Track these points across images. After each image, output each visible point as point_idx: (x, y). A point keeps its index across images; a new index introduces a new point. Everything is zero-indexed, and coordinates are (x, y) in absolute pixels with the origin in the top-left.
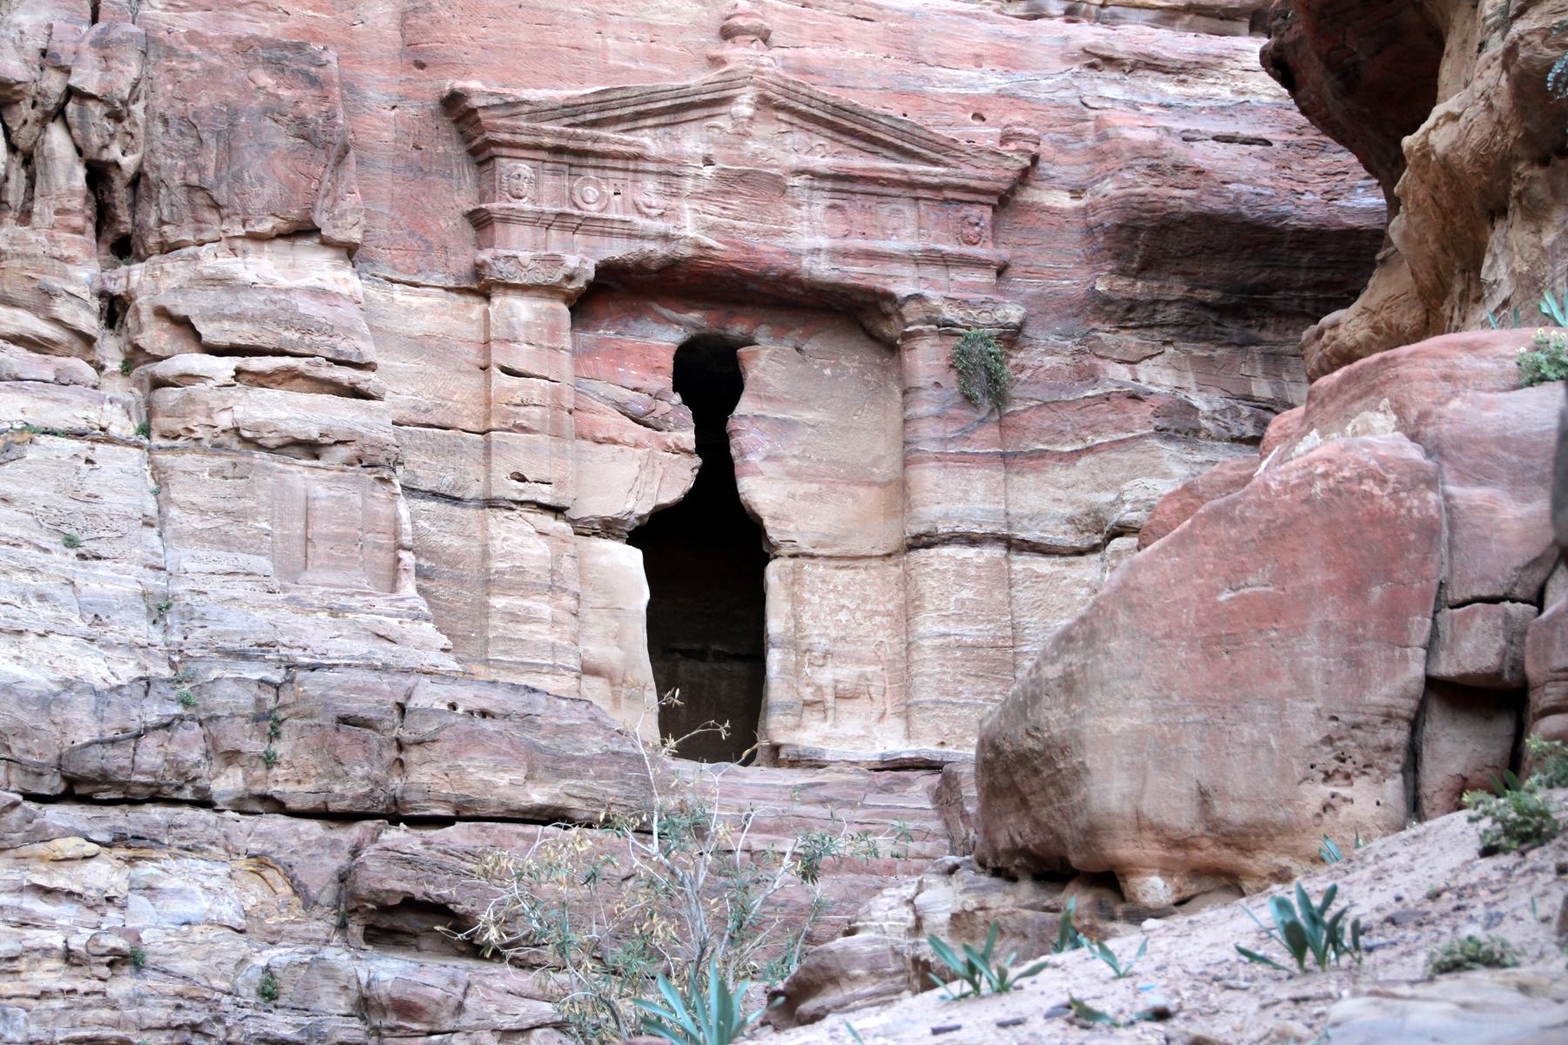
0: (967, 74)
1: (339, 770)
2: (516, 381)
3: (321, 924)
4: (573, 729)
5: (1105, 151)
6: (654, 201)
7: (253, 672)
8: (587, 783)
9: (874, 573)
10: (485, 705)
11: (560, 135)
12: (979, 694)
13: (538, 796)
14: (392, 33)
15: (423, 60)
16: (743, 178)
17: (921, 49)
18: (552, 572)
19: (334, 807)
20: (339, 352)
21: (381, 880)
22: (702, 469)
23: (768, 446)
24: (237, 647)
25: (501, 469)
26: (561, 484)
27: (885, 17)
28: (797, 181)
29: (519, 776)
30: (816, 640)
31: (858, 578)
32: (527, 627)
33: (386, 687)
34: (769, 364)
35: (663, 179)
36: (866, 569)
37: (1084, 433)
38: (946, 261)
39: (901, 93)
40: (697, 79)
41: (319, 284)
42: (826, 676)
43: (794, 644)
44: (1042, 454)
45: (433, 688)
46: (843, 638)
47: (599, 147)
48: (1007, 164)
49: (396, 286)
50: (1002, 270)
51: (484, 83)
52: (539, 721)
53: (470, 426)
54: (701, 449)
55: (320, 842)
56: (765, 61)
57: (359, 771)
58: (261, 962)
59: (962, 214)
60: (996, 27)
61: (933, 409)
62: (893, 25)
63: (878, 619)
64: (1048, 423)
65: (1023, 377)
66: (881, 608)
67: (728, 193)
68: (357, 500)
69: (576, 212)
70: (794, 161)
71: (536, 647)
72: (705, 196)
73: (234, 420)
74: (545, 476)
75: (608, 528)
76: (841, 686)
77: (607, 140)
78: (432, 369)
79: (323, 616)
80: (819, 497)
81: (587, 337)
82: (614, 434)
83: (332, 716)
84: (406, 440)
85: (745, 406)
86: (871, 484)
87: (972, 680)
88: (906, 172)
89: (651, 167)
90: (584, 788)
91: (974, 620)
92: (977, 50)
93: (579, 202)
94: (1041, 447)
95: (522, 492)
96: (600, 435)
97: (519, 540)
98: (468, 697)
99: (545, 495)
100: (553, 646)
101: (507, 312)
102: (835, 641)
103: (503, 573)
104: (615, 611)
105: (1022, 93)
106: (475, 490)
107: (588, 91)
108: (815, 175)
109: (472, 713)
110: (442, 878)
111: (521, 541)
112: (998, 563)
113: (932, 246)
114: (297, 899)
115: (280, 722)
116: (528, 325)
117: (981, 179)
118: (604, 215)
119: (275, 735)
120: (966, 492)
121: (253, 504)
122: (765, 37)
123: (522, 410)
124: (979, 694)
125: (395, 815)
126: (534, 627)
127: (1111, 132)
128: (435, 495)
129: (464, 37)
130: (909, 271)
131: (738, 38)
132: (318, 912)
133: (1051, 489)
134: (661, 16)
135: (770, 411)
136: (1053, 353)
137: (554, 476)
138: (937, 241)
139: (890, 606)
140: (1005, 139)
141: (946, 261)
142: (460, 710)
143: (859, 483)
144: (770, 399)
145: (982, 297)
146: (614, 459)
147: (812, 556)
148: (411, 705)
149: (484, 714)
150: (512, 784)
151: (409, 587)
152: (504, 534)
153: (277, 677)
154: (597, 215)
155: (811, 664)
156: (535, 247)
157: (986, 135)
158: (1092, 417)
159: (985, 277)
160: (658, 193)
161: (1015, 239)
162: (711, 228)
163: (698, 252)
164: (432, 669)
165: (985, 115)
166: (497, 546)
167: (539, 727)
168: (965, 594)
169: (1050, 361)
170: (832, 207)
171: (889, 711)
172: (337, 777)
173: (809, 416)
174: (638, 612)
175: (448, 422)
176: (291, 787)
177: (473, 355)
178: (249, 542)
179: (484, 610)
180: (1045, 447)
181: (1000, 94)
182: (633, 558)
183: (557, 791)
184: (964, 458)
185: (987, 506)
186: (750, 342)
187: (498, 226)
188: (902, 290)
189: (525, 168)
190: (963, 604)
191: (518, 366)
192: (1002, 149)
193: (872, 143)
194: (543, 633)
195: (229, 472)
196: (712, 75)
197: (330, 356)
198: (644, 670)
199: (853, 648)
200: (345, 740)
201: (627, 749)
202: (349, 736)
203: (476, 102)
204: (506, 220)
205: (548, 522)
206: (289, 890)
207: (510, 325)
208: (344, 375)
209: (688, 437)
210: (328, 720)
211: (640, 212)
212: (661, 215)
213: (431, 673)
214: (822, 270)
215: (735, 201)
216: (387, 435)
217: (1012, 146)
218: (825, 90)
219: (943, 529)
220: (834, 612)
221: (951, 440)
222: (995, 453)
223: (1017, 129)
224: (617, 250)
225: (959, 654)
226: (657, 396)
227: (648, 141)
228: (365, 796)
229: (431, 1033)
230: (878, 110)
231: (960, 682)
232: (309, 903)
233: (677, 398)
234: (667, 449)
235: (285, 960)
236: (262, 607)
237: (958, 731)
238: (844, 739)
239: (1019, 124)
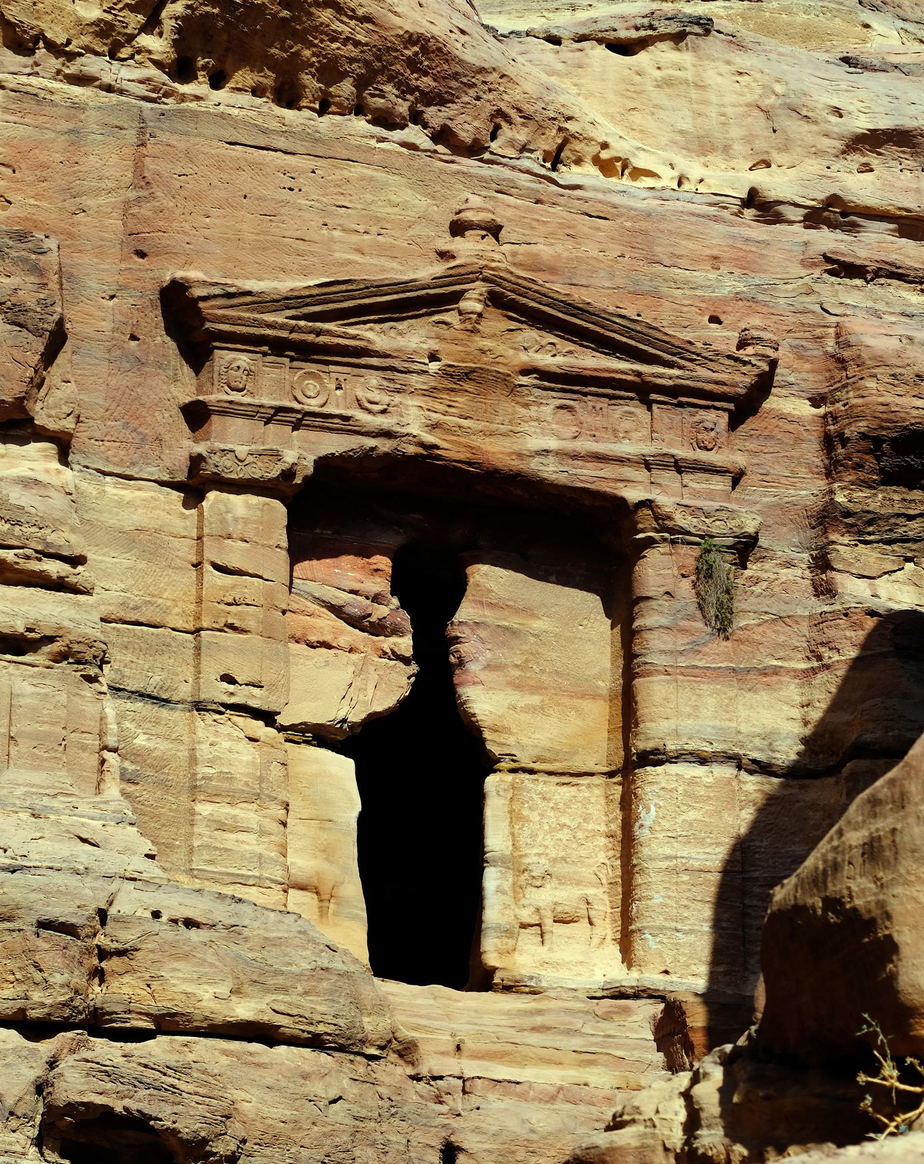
0: (704, 275)
1: (38, 976)
2: (229, 579)
4: (277, 943)
5: (844, 361)
6: (376, 396)
8: (293, 998)
9: (597, 791)
11: (282, 327)
13: (244, 1010)
14: (115, 223)
15: (145, 249)
16: (467, 375)
17: (658, 249)
18: (261, 779)
20: (48, 545)
21: (81, 1093)
23: (489, 655)
25: (212, 670)
27: (622, 215)
28: (524, 380)
29: (223, 990)
30: (535, 859)
32: (233, 836)
33: (88, 892)
35: (389, 374)
36: (589, 786)
37: (822, 649)
38: (679, 466)
39: (635, 293)
40: (426, 271)
41: (30, 474)
42: (546, 897)
44: (776, 671)
45: (136, 894)
46: (564, 859)
47: (322, 339)
48: (745, 369)
49: (108, 478)
50: (737, 478)
51: (206, 273)
52: (246, 932)
53: (179, 624)
54: (420, 654)
56: (497, 256)
57: (58, 979)
59: (697, 418)
60: (735, 230)
62: (628, 224)
64: (782, 638)
65: (757, 589)
67: (452, 390)
68: (63, 698)
69: (296, 405)
70: (524, 358)
71: (242, 857)
72: (431, 392)
74: (255, 678)
75: (321, 736)
77: (329, 333)
78: (142, 565)
79: (25, 816)
80: (541, 709)
82: (328, 638)
84: (113, 638)
85: (466, 612)
88: (639, 374)
89: (374, 361)
91: (701, 842)
92: (715, 252)
94: (776, 663)
96: (313, 638)
97: (227, 744)
98: (174, 905)
100: (260, 857)
101: (222, 508)
102: (555, 860)
103: (210, 779)
105: (760, 297)
106: (184, 691)
107: (312, 283)
108: (544, 375)
109: (175, 921)
110: (142, 1093)
111: (231, 747)
112: (729, 783)
113: (665, 450)
117: (717, 383)
118: (325, 410)
120: (696, 708)
122: (494, 230)
123: (233, 609)
125: (98, 1024)
126: (242, 836)
127: (853, 340)
128: (143, 695)
129: (187, 226)
130: (641, 475)
131: (467, 233)
133: (786, 708)
134: (390, 210)
135: (489, 616)
138: (670, 445)
140: (742, 345)
141: (679, 466)
142: (164, 918)
143: (583, 696)
144: (492, 605)
145: (716, 505)
146: (327, 663)
147: (532, 772)
148: (112, 911)
149: (189, 923)
151: (113, 789)
152: (212, 739)
154: (317, 410)
157: (723, 338)
159: (720, 484)
160: (381, 388)
161: (751, 445)
162: (435, 427)
163: (420, 450)
164: (136, 875)
165: (722, 318)
166: (204, 751)
167: (246, 939)
168: (692, 815)
169: (786, 574)
170: (561, 407)
175: (157, 619)
177: (186, 551)
179: (191, 818)
180: (779, 663)
181: (738, 297)
182: (341, 769)
183: (264, 1006)
184: (694, 672)
185: (718, 723)
187: (215, 418)
188: (633, 495)
189: (244, 359)
190: (691, 825)
192: (741, 354)
194: (250, 843)
196: (439, 268)
197: (39, 548)
198: (353, 889)
199: (573, 868)
200: (46, 946)
201: (338, 965)
203: (197, 292)
204: (223, 413)
205: (258, 727)
208: (54, 568)
209: (405, 644)
210: (27, 922)
211: (362, 407)
212: (384, 412)
213: (134, 879)
214: (550, 471)
215: (461, 400)
216: (92, 629)
217: (750, 350)
218: (559, 288)
219: (672, 746)
220: (552, 830)
221: (681, 653)
222: (728, 668)
223: (755, 333)
224: (335, 444)
225: (685, 878)
226: (377, 599)
228: (65, 1005)
230: (612, 309)
233: (395, 601)
234: (384, 654)
237: (683, 959)
239: (756, 328)
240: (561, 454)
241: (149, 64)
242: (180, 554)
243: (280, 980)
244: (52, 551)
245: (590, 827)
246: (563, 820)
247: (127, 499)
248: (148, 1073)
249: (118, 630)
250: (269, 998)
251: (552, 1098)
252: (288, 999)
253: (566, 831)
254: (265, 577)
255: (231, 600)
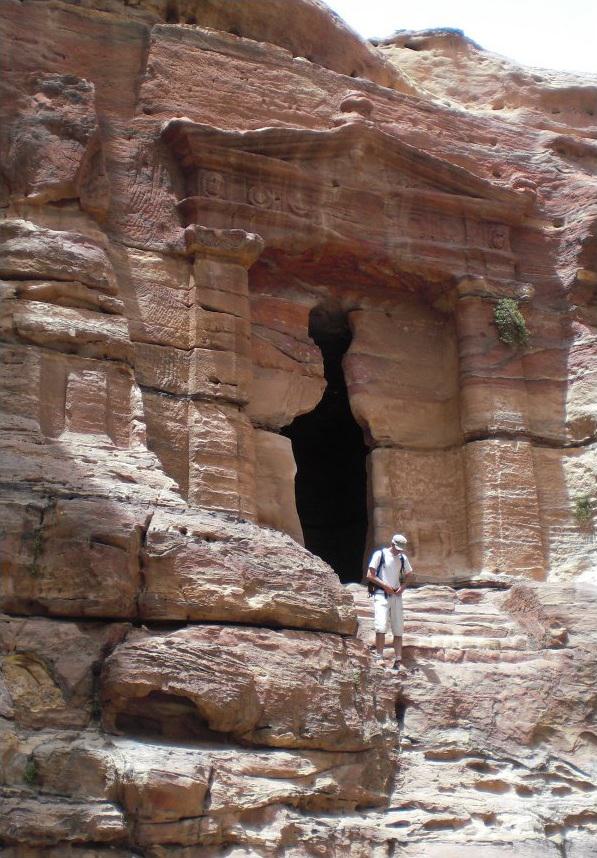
1: (93, 581)
3: (79, 711)
7: (23, 499)
10: (209, 529)
12: (519, 537)
13: (255, 603)
19: (92, 611)
20: (92, 280)
22: (328, 388)
24: (9, 480)
26: (243, 386)
31: (429, 462)
34: (369, 324)
37: (575, 368)
43: (391, 503)
45: (168, 516)
46: (422, 501)
54: (328, 375)
55: (76, 641)
57: (110, 582)
58: (26, 750)
59: (493, 229)
61: (481, 350)
63: (443, 489)
66: (444, 482)
72: (334, 206)
73: (15, 323)
76: (422, 532)
81: (255, 296)
83: (87, 534)
85: (355, 348)
86: (436, 401)
87: (514, 528)
90: (289, 597)
93: (253, 201)
95: (216, 391)
99: (233, 393)
102: (416, 503)
104: (275, 479)
110: (183, 675)
114: (58, 690)
115: (46, 540)
116: (218, 278)
119: (39, 552)
121: (26, 381)
124: (519, 537)
129: (177, 96)
130: (461, 263)
132: (76, 701)
133: (554, 405)
136: (550, 320)
137: (240, 380)
139: (451, 480)
142: (189, 534)
145: (508, 281)
147: (401, 448)
150: (234, 595)
153: (43, 503)
155: (403, 518)
156: (224, 227)
158: (581, 358)
159: (508, 270)
164: (165, 503)
167: (252, 549)
168: (507, 471)
171: (454, 550)
172: (92, 587)
173: (395, 356)
174: (290, 480)
176: (54, 595)
178: (22, 409)
182: (285, 445)
184: (501, 382)
186: (357, 309)
191: (214, 304)
193: (438, 184)
195: (9, 359)
197: (85, 281)
200: (99, 556)
202: (101, 551)
206: (51, 682)
207: (208, 277)
211: (292, 211)
213: (165, 506)
220: (415, 484)
221: (494, 370)
222: (521, 380)
224: (278, 236)
227: (297, 168)
229: (182, 819)
231: (507, 529)
232: (70, 695)
235: (50, 748)
236: (31, 453)
238: (427, 568)
240: (416, 249)
241: (149, 7)
242: (178, 299)
243: (279, 579)
244: (94, 284)
245: (437, 481)
246: (422, 477)
247: (143, 262)
248: (188, 657)
249: (139, 346)
250: (274, 593)
251: (460, 660)
252: (286, 593)
253: (422, 484)
254: (236, 313)
255: (213, 328)
